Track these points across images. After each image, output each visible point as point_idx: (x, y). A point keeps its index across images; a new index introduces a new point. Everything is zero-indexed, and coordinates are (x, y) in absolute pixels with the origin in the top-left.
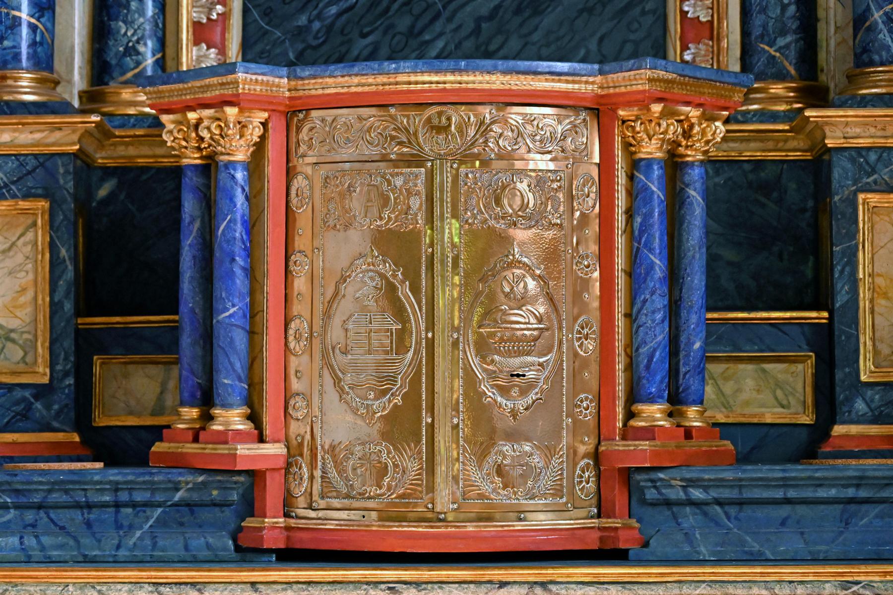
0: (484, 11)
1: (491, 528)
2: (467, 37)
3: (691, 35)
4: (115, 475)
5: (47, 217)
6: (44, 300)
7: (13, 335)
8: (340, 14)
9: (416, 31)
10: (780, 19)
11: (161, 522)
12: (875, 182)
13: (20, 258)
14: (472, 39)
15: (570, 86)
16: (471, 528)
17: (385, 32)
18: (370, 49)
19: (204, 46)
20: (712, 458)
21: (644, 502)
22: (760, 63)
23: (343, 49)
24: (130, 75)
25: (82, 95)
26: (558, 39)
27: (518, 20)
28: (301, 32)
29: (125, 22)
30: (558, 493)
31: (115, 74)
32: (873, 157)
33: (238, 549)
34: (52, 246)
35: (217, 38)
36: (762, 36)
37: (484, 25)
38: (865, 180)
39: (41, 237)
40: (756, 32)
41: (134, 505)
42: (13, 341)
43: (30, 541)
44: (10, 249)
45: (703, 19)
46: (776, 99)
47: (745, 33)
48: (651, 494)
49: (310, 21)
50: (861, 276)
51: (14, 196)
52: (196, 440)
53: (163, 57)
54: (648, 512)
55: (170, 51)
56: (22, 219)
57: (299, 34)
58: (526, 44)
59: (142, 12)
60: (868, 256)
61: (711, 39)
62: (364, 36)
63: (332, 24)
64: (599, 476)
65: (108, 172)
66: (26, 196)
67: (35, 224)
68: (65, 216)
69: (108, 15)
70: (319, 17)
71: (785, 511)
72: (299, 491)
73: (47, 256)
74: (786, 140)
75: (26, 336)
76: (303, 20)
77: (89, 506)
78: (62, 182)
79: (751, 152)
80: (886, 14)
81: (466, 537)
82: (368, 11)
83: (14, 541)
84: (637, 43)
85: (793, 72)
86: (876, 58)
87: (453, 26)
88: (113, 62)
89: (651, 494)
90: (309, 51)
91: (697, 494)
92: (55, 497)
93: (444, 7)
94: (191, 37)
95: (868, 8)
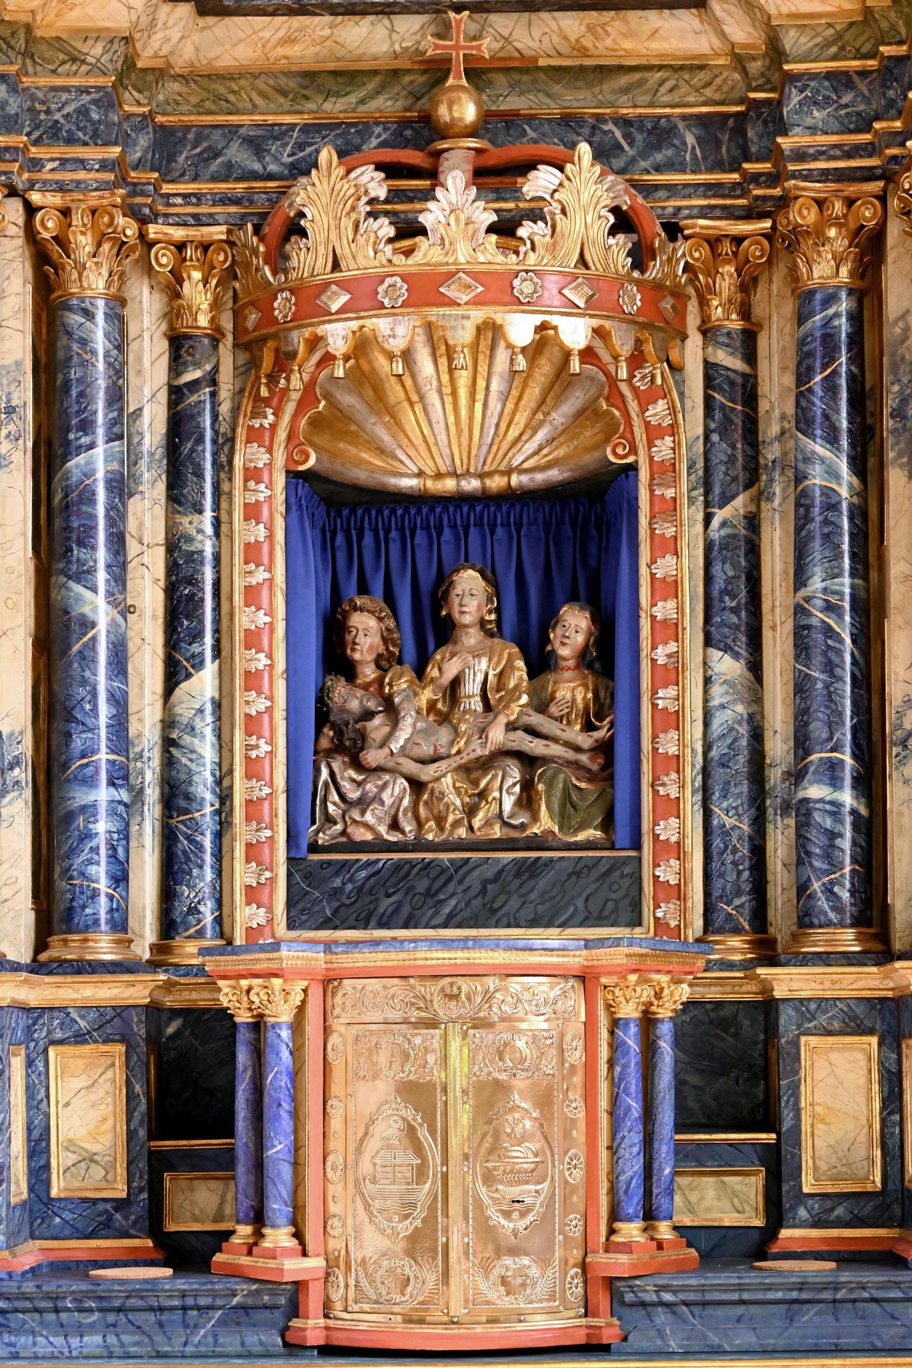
0: (490, 875)
1: (496, 1329)
2: (475, 897)
3: (661, 896)
4: (182, 1284)
5: (123, 1058)
6: (122, 1128)
7: (96, 1158)
8: (368, 878)
9: (433, 891)
10: (736, 883)
11: (221, 1322)
12: (815, 1027)
13: (101, 1093)
14: (480, 898)
15: (560, 959)
16: (479, 1329)
17: (407, 893)
18: (394, 906)
19: (254, 905)
20: (681, 1268)
21: (623, 1303)
22: (719, 920)
23: (372, 907)
24: (192, 931)
25: (152, 947)
26: (552, 898)
27: (517, 882)
28: (335, 893)
29: (187, 886)
30: (552, 1298)
31: (180, 930)
32: (813, 1006)
33: (286, 1344)
34: (128, 1083)
35: (266, 900)
36: (722, 896)
37: (490, 887)
38: (807, 1025)
39: (119, 1074)
40: (716, 893)
41: (199, 1308)
42: (96, 1162)
43: (112, 1339)
44: (92, 1085)
45: (672, 882)
46: (733, 950)
47: (707, 894)
48: (629, 1297)
49: (344, 884)
50: (803, 1105)
51: (96, 1042)
52: (250, 1253)
53: (221, 915)
54: (626, 1312)
55: (226, 910)
56: (102, 1060)
57: (334, 894)
58: (524, 903)
59: (202, 878)
60: (809, 1089)
61: (679, 899)
62: (389, 896)
63: (363, 885)
64: (586, 1282)
65: (175, 1013)
66: (106, 1041)
67: (113, 1065)
68: (139, 1058)
69: (174, 879)
70: (351, 880)
71: (740, 1310)
72: (337, 1296)
73: (124, 1091)
74: (741, 986)
75: (106, 1158)
76: (337, 882)
77: (161, 1309)
78: (136, 1029)
79: (713, 994)
80: (824, 884)
81: (476, 1337)
82: (393, 873)
83: (98, 1339)
84: (616, 902)
85: (747, 927)
86: (816, 921)
87: (463, 887)
88: (179, 920)
89: (629, 1297)
90: (342, 909)
91: (667, 1297)
92: (133, 1302)
93: (456, 872)
94: (244, 898)
95: (809, 879)
